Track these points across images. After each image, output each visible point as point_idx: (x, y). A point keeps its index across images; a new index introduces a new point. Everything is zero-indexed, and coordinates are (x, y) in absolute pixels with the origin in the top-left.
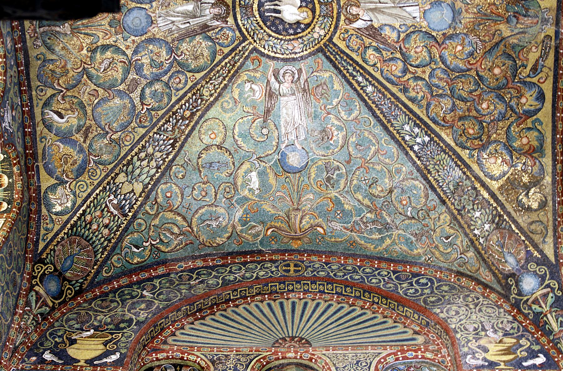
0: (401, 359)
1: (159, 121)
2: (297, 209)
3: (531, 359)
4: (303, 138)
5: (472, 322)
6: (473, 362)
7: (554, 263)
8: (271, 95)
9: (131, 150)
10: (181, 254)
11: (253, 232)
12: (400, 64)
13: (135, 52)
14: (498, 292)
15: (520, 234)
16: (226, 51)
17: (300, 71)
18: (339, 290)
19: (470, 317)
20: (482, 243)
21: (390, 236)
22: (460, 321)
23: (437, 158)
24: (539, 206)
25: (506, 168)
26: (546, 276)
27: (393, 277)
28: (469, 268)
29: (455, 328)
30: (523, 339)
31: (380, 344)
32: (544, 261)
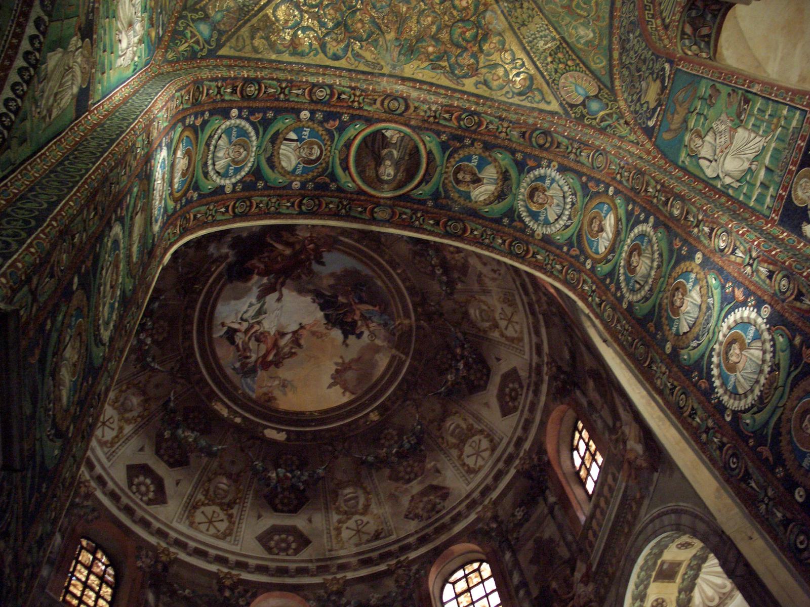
32: (220, 46)
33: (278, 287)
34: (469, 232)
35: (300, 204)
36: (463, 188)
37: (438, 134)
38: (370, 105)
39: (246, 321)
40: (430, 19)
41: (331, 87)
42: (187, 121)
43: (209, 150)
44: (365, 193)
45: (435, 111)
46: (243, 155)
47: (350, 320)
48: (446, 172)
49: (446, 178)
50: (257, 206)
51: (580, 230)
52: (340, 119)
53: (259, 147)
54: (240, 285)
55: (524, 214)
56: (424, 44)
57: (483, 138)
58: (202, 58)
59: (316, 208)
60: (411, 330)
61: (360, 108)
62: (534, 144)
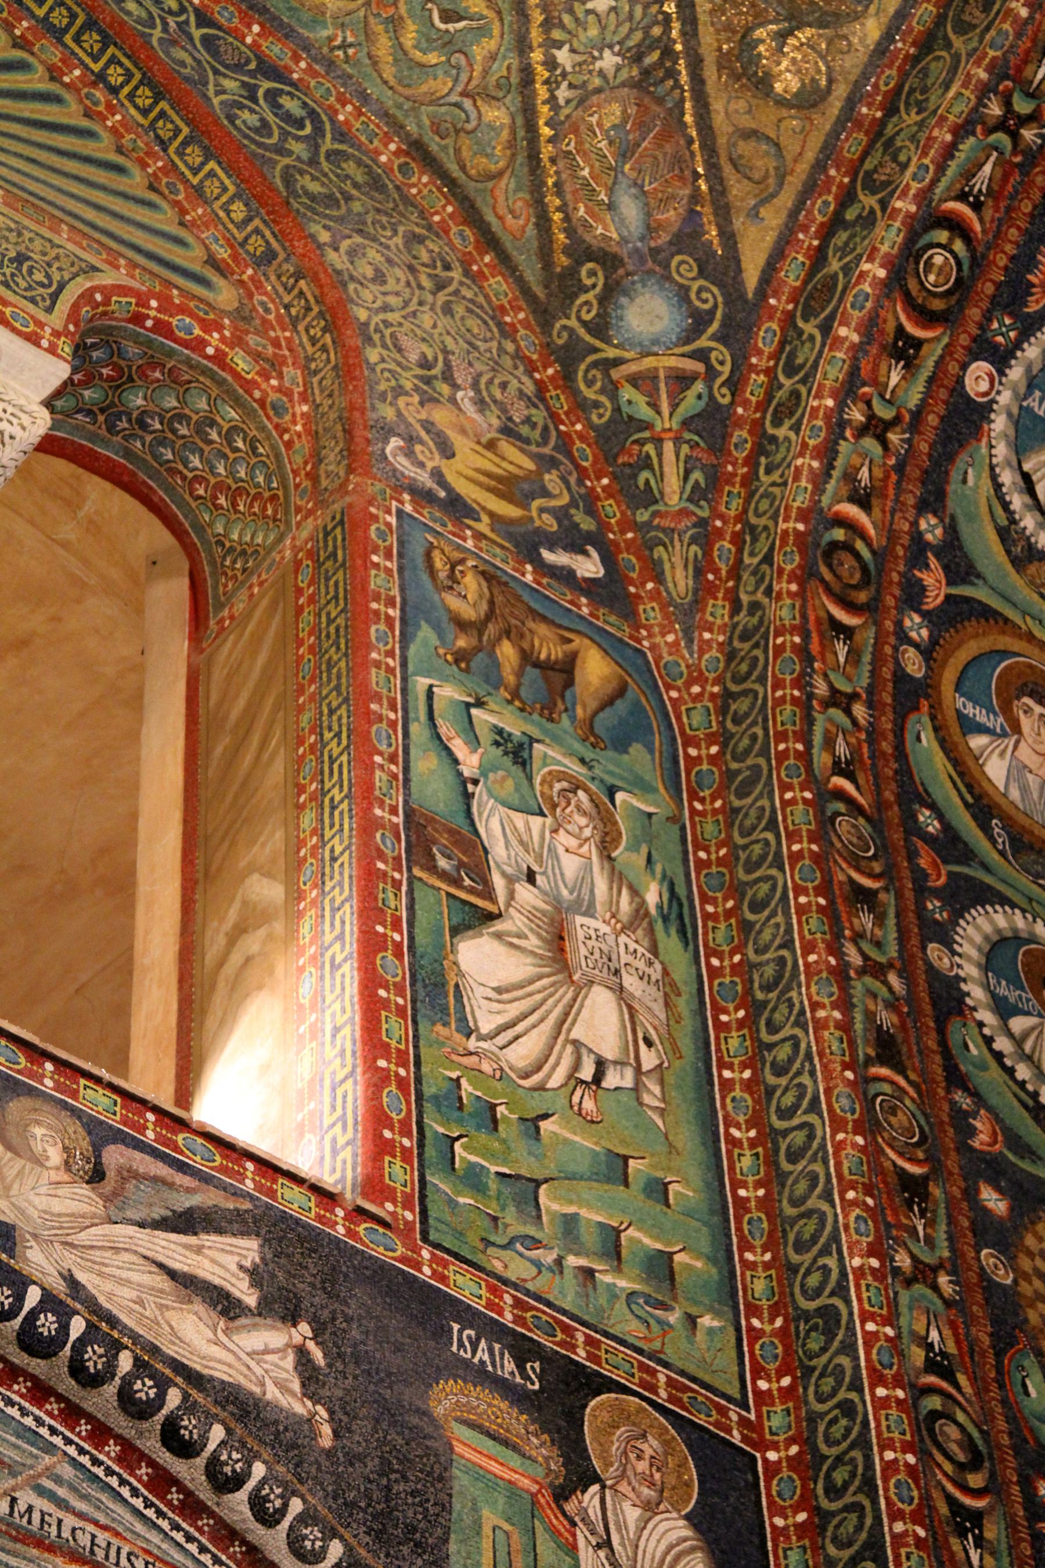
0: (149, 323)
3: (565, 549)
5: (419, 332)
6: (402, 463)
7: (750, 295)
14: (521, 283)
15: (696, 146)
19: (414, 314)
20: (561, 102)
22: (386, 308)
24: (796, 95)
26: (711, 322)
27: (197, 33)
28: (465, 154)
29: (366, 324)
30: (554, 472)
31: (97, 235)
42: (913, 664)
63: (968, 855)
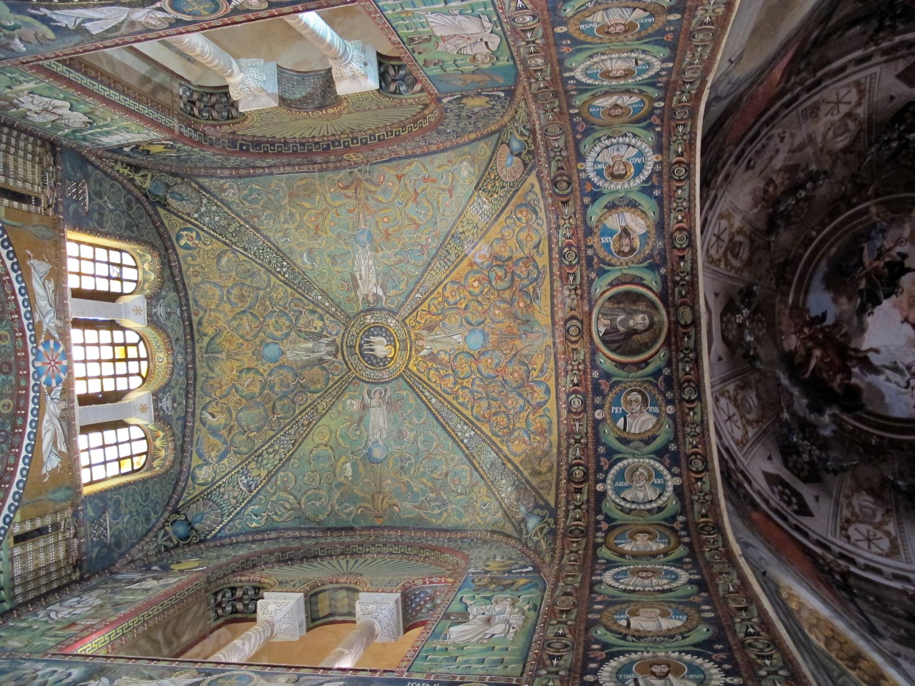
1: (285, 426)
2: (380, 492)
4: (385, 436)
8: (364, 407)
9: (262, 446)
10: (291, 524)
11: (347, 511)
12: (452, 378)
13: (270, 374)
16: (337, 378)
17: (386, 391)
18: (403, 550)
21: (446, 511)
23: (479, 446)
25: (523, 446)
32: (547, 506)
33: (861, 355)
34: (681, 224)
35: (690, 401)
36: (637, 243)
37: (591, 282)
38: (578, 352)
39: (908, 383)
40: (497, 312)
41: (568, 395)
42: (600, 540)
43: (635, 509)
44: (668, 338)
45: (570, 290)
46: (643, 471)
47: (886, 271)
48: (627, 264)
49: (633, 262)
50: (696, 447)
51: (629, 123)
52: (597, 379)
53: (634, 456)
54: (865, 395)
55: (642, 178)
56: (519, 311)
57: (582, 238)
58: (556, 523)
59: (692, 384)
60: (882, 203)
61: (584, 361)
62: (569, 190)
63: (615, 562)
